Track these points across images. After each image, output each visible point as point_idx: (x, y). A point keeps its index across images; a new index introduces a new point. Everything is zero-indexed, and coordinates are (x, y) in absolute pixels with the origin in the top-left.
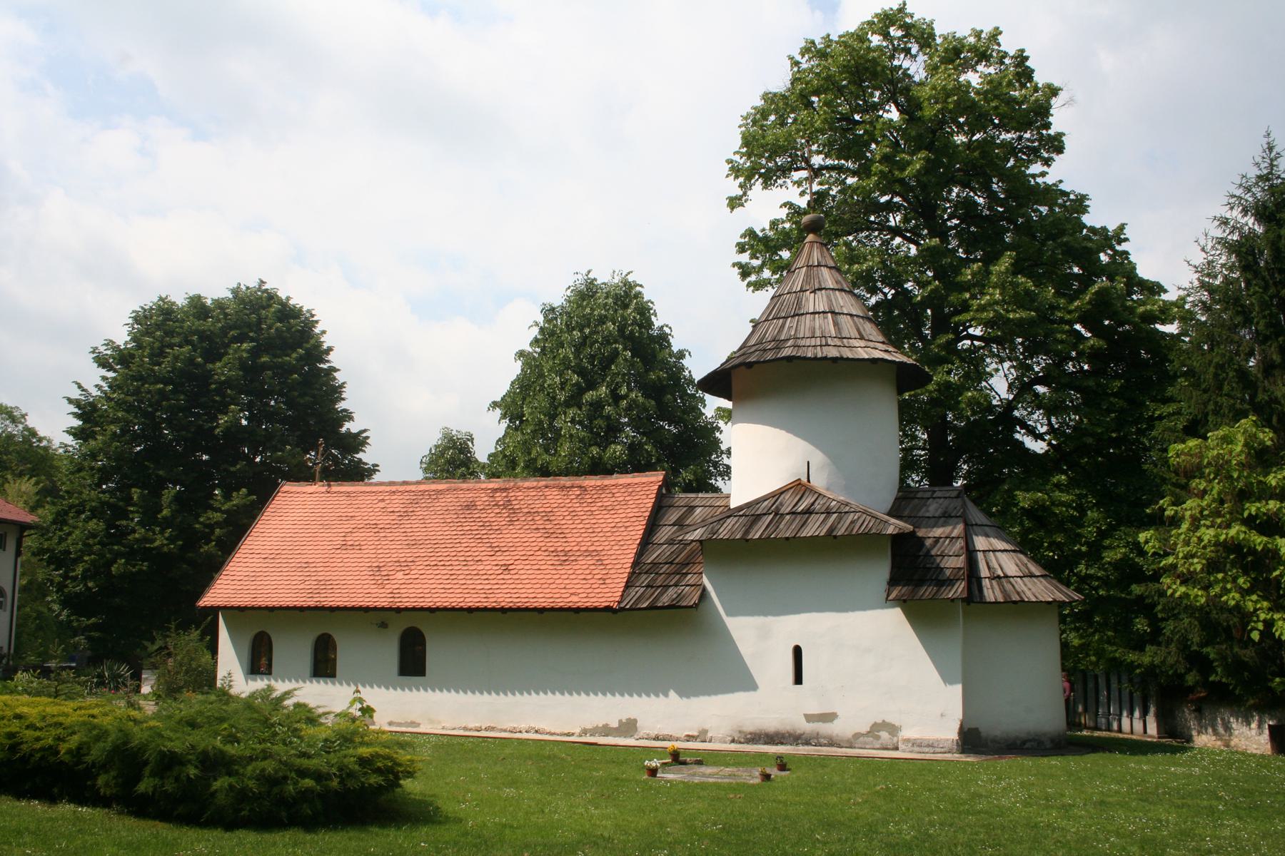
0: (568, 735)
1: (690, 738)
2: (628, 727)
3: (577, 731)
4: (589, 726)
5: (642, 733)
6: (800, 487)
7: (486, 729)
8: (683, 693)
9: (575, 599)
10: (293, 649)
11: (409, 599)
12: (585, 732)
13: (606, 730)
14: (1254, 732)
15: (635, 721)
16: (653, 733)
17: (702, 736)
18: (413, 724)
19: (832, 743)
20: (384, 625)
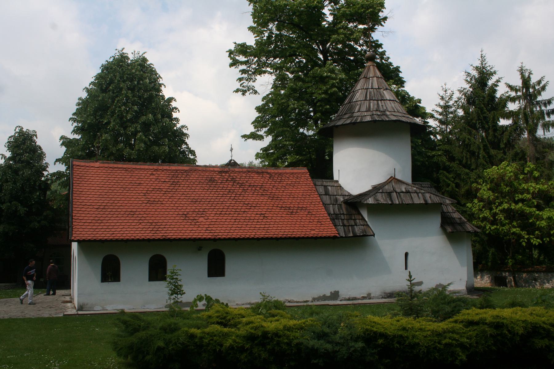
1: (364, 298)
2: (335, 295)
3: (310, 299)
4: (316, 297)
5: (341, 298)
6: (393, 179)
9: (313, 232)
11: (222, 232)
12: (314, 299)
13: (324, 298)
14: (479, 280)
15: (338, 292)
16: (347, 297)
17: (369, 296)
20: (200, 249)
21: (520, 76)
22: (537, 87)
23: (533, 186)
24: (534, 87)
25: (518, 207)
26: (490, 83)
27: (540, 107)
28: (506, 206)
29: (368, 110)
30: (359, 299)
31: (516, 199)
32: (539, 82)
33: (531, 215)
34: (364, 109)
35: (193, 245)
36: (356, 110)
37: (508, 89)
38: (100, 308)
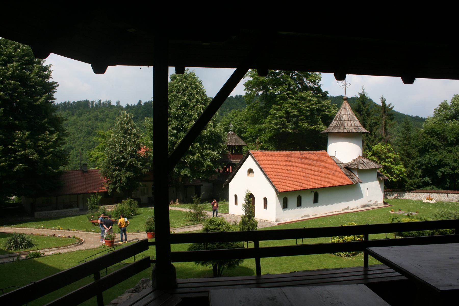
2: (348, 208)
5: (350, 208)
8: (355, 200)
10: (292, 201)
13: (345, 209)
18: (316, 215)
19: (371, 206)
23: (392, 155)
25: (388, 165)
28: (383, 164)
29: (351, 126)
30: (353, 209)
32: (389, 105)
33: (392, 168)
34: (349, 125)
35: (312, 190)
36: (346, 125)
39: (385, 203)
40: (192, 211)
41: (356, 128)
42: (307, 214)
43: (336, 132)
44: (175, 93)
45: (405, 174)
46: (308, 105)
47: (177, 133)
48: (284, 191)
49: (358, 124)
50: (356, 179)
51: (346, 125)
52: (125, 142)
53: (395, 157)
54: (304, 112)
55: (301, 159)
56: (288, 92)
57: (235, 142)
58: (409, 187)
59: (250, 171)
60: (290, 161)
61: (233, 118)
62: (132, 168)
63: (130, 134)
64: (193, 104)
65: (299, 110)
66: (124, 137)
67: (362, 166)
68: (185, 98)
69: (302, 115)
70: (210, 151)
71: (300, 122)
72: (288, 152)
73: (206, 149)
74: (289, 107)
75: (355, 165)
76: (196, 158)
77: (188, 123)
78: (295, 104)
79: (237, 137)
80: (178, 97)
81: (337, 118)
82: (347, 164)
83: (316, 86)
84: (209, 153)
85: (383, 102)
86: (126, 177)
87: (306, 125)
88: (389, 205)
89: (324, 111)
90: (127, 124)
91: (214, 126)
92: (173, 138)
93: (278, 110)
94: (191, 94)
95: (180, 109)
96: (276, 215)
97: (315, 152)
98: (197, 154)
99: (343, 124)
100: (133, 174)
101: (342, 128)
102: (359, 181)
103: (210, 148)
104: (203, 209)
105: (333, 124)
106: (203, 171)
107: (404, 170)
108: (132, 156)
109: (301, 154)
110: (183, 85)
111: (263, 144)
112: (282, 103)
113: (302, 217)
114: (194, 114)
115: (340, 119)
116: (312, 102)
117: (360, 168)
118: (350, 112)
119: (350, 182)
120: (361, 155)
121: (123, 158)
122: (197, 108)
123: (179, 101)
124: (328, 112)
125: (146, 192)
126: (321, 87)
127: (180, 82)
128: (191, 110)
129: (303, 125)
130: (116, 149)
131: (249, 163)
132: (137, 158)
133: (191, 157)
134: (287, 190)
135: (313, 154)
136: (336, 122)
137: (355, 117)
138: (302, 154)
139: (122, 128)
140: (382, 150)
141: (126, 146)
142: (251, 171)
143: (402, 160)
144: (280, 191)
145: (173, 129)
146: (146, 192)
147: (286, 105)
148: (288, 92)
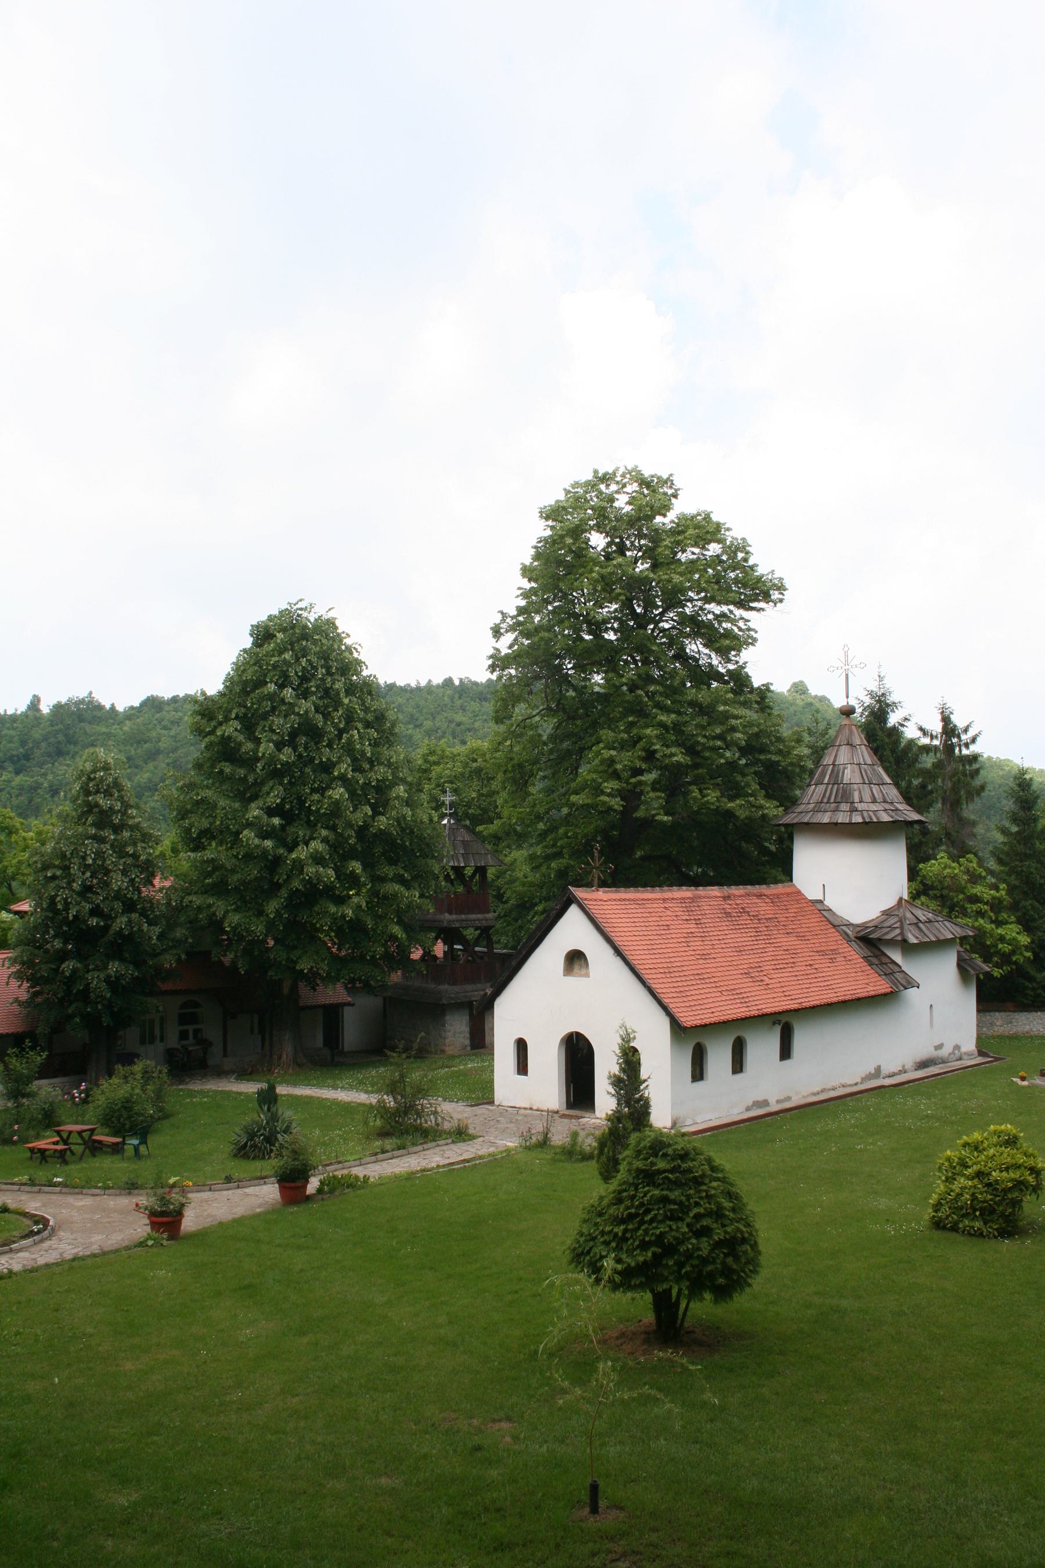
0: (856, 1084)
1: (900, 1072)
3: (859, 1080)
5: (883, 1074)
7: (822, 1091)
12: (864, 1079)
18: (789, 1099)
21: (939, 717)
22: (963, 737)
24: (959, 737)
26: (893, 719)
27: (964, 765)
31: (969, 910)
34: (867, 798)
36: (857, 799)
37: (919, 734)
38: (689, 1122)
39: (981, 1053)
40: (390, 1101)
41: (887, 806)
42: (760, 1098)
43: (826, 820)
44: (272, 687)
45: (1028, 954)
46: (718, 731)
47: (283, 827)
48: (698, 1023)
49: (893, 793)
50: (898, 976)
51: (857, 799)
52: (99, 855)
53: (993, 898)
54: (707, 754)
55: (728, 914)
56: (652, 688)
57: (465, 856)
58: (1039, 995)
59: (575, 959)
60: (698, 922)
61: (425, 771)
62: (125, 946)
63: (117, 829)
64: (335, 726)
65: (691, 750)
66: (94, 837)
67: (917, 933)
68: (305, 706)
69: (696, 766)
70: (397, 887)
71: (693, 788)
72: (686, 892)
73: (383, 880)
74: (657, 737)
75: (892, 928)
76: (350, 912)
77: (322, 791)
78: (677, 728)
79: (467, 838)
80: (283, 700)
81: (823, 774)
82: (864, 926)
83: (731, 667)
84: (395, 896)
85: (946, 720)
86: (108, 980)
87: (712, 796)
88: (997, 1059)
89: (763, 750)
90: (108, 793)
91: (408, 803)
92: (268, 843)
93: (623, 746)
94: (327, 692)
95: (292, 743)
96: (674, 1105)
97: (763, 889)
98: (355, 900)
99: (845, 796)
100: (130, 972)
101: (844, 807)
102: (909, 983)
103: (401, 880)
104: (421, 1091)
105: (814, 793)
106: (373, 957)
107: (1024, 939)
108: (130, 906)
109: (726, 898)
110: (297, 659)
111: (563, 862)
112: (632, 724)
113: (748, 1109)
114: (340, 760)
115: (836, 778)
116: (733, 722)
117: (913, 940)
118: (865, 755)
119: (882, 986)
120: (906, 897)
121: (95, 912)
122: (350, 742)
123: (286, 716)
124: (780, 752)
125: (157, 1032)
126: (749, 670)
127: (286, 650)
128: (330, 745)
129: (704, 796)
130: (69, 883)
131: (572, 930)
132: (143, 913)
133: (333, 909)
134: (707, 1021)
135: (760, 896)
136: (822, 787)
137: (880, 770)
138: (729, 897)
139: (91, 807)
140: (954, 877)
141: (107, 872)
142: (575, 959)
143: (1014, 907)
144: (688, 1024)
145: (271, 812)
146: (157, 1032)
147: (648, 731)
148: (652, 688)
